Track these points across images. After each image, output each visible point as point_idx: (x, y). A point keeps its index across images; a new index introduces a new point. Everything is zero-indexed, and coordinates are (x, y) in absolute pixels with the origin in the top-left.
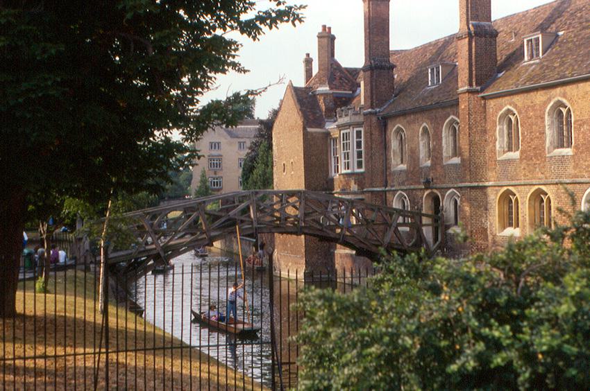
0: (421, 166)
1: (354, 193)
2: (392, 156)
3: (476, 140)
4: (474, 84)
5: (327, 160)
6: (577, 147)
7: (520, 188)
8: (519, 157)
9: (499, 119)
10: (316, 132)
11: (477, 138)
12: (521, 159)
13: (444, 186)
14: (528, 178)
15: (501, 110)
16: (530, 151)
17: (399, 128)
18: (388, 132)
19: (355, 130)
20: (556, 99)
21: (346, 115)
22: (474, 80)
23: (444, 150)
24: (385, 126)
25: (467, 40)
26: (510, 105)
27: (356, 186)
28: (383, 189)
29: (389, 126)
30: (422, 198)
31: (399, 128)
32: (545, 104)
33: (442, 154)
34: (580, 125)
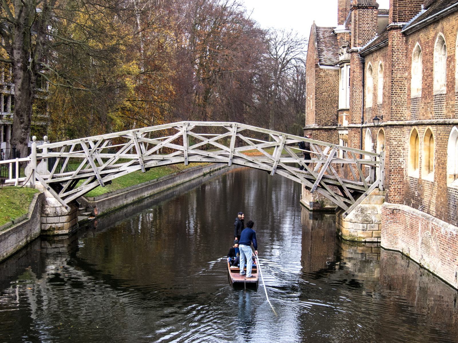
0: (378, 104)
1: (345, 129)
6: (447, 86)
7: (421, 128)
8: (421, 96)
9: (414, 55)
10: (328, 70)
11: (399, 76)
12: (422, 98)
15: (414, 46)
18: (365, 70)
19: (349, 67)
24: (363, 63)
27: (347, 121)
28: (360, 125)
29: (366, 63)
31: (370, 66)
32: (434, 38)
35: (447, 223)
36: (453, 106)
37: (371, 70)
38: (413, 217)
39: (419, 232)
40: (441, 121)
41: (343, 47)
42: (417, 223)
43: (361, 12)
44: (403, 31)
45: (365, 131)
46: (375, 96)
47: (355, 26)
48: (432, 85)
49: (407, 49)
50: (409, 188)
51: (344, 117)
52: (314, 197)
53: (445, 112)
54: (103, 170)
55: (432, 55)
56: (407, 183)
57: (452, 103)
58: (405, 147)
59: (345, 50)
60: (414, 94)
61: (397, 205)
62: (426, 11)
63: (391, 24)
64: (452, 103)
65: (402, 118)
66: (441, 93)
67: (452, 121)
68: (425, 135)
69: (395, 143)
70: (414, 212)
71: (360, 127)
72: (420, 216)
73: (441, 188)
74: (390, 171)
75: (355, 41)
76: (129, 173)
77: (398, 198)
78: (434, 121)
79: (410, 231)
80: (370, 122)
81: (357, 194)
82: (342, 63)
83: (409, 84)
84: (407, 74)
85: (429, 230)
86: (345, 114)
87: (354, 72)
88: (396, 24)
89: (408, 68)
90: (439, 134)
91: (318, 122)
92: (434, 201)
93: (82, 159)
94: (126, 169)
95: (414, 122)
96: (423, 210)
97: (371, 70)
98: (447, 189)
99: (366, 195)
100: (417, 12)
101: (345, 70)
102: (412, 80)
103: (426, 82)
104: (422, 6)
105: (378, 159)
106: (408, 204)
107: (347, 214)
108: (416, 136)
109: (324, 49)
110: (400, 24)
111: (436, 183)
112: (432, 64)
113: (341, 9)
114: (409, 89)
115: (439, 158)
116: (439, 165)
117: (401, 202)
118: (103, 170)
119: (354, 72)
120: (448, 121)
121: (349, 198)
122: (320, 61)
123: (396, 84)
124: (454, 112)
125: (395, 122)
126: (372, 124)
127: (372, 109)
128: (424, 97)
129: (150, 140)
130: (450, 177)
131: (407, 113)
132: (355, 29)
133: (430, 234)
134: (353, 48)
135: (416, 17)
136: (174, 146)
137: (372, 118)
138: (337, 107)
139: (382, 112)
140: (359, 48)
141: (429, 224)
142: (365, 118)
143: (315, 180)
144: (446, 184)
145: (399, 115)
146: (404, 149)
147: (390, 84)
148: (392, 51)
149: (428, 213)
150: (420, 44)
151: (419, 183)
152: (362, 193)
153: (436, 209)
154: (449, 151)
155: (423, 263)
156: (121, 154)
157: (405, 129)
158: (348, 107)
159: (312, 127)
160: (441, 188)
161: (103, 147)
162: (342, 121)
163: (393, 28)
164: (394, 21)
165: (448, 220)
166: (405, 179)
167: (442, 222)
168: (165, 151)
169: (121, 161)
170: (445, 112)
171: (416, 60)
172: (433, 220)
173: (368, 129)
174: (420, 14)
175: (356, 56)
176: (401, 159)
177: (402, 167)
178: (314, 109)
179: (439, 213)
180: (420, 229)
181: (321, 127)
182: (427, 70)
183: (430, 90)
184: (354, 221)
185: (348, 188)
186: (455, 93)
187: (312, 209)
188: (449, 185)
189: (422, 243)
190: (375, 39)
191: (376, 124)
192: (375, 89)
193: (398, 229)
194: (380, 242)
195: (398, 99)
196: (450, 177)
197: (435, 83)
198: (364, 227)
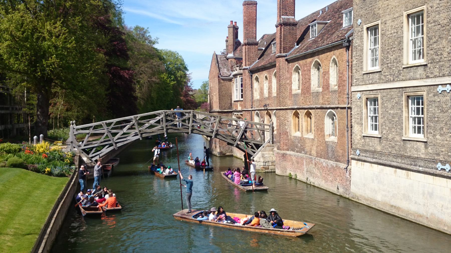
2: (254, 92)
3: (283, 84)
4: (282, 52)
5: (231, 93)
7: (301, 110)
11: (284, 82)
12: (301, 94)
13: (273, 108)
14: (304, 104)
15: (294, 67)
16: (305, 89)
17: (257, 76)
20: (315, 60)
21: (236, 70)
22: (282, 50)
23: (273, 89)
24: (252, 76)
25: (279, 27)
26: (298, 64)
30: (264, 114)
31: (257, 76)
32: (311, 63)
33: (272, 91)
34: (325, 75)
35: (327, 160)
36: (328, 98)
37: (257, 79)
38: (297, 157)
39: (305, 165)
40: (319, 106)
41: (237, 66)
42: (302, 160)
43: (249, 47)
44: (286, 58)
45: (255, 113)
46: (262, 93)
47: (246, 55)
48: (310, 87)
49: (288, 68)
50: (293, 142)
51: (239, 105)
52: (220, 149)
53: (321, 101)
54: (117, 139)
55: (310, 71)
56: (291, 139)
57: (327, 96)
58: (289, 120)
59: (238, 68)
60: (294, 92)
61: (285, 151)
62: (298, 46)
63: (279, 54)
64: (327, 96)
65: (286, 105)
66: (318, 91)
67: (328, 106)
68: (305, 114)
69: (282, 118)
70: (299, 155)
71: (250, 111)
72: (304, 157)
73: (320, 141)
74: (280, 133)
75: (246, 63)
76: (133, 140)
77: (285, 147)
78: (314, 106)
79: (296, 165)
80: (258, 107)
81: (258, 146)
82: (235, 76)
83: (290, 86)
84: (288, 81)
85: (313, 164)
86: (239, 103)
87: (245, 80)
88: (282, 54)
89: (291, 78)
90: (317, 113)
91: (220, 108)
92: (314, 148)
93: (104, 134)
94: (131, 138)
95: (296, 107)
96: (306, 154)
97: (257, 79)
98: (326, 142)
99: (264, 147)
100: (293, 47)
101: (239, 78)
102: (293, 85)
103: (305, 86)
104: (296, 44)
105: (266, 127)
106: (293, 150)
107: (254, 158)
108: (296, 115)
109: (222, 67)
110: (285, 54)
111: (316, 139)
112: (310, 76)
113: (230, 44)
114: (291, 89)
115: (318, 126)
116: (318, 130)
117: (288, 150)
118: (117, 139)
119: (245, 80)
120: (324, 106)
121: (254, 149)
122: (220, 74)
123: (283, 87)
124: (328, 101)
125: (282, 108)
126: (263, 108)
127: (260, 101)
128: (303, 93)
129: (140, 121)
130: (327, 136)
131: (289, 102)
132: (246, 56)
133: (314, 166)
134: (244, 67)
135: (292, 50)
136: (158, 124)
137: (259, 105)
138: (231, 99)
139: (268, 102)
140: (248, 67)
141: (312, 161)
142: (253, 105)
143: (236, 140)
144: (324, 139)
145: (284, 104)
146: (288, 122)
147: (279, 87)
148: (280, 69)
149: (310, 155)
150: (300, 65)
151: (302, 140)
152: (260, 146)
153: (316, 152)
154: (325, 122)
155: (308, 182)
156: (125, 130)
157: (288, 111)
158: (242, 99)
159: (217, 111)
160: (320, 141)
161: (112, 126)
162: (237, 107)
163: (279, 57)
164: (281, 53)
165: (328, 158)
166: (289, 137)
167: (322, 160)
168: (151, 126)
169: (124, 134)
170: (321, 101)
171: (295, 74)
172: (315, 159)
173: (256, 111)
174: (294, 48)
175: (247, 71)
176: (286, 127)
177: (287, 131)
178: (218, 101)
179: (319, 155)
180: (304, 164)
181: (222, 111)
182: (305, 79)
183: (308, 90)
184: (258, 161)
185: (254, 144)
186: (329, 91)
187: (219, 156)
188: (327, 140)
189: (307, 171)
190: (257, 61)
191: (265, 108)
192: (262, 90)
193: (288, 164)
194: (275, 172)
195: (284, 95)
196: (327, 136)
197: (312, 86)
198: (264, 164)
